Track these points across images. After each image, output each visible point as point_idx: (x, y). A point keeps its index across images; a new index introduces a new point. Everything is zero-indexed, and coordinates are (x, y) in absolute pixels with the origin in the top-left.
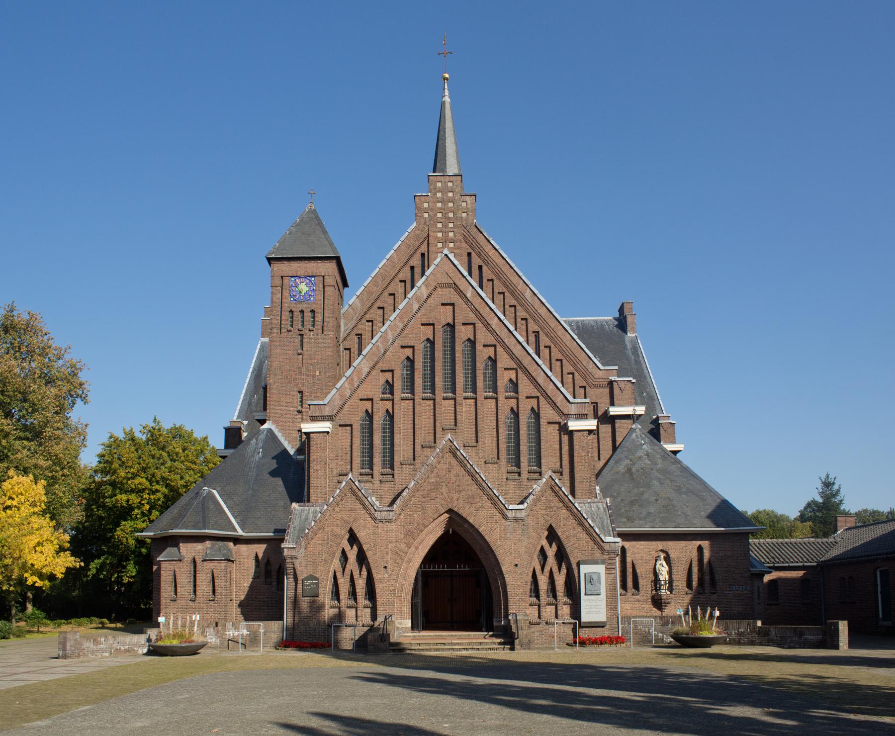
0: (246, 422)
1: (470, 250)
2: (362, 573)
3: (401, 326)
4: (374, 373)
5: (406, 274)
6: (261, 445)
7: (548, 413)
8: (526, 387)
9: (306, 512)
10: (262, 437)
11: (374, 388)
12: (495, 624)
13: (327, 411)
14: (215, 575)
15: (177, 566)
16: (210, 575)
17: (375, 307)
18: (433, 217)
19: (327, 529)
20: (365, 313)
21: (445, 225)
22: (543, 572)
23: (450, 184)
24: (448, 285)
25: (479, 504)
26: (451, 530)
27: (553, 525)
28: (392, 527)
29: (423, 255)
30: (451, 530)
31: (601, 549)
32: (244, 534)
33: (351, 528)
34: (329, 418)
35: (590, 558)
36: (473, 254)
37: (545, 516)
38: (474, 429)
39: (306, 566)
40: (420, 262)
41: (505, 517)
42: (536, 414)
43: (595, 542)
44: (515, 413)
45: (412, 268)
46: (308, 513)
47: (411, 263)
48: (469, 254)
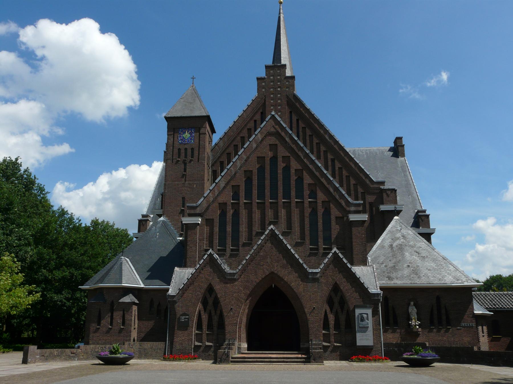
0: (152, 216)
5: (251, 125)
7: (335, 212)
9: (183, 273)
10: (159, 225)
12: (301, 346)
13: (198, 211)
20: (226, 149)
26: (273, 285)
27: (337, 282)
29: (262, 113)
30: (273, 285)
32: (144, 287)
37: (332, 277)
40: (259, 117)
42: (327, 213)
45: (255, 121)
46: (185, 274)
47: (255, 118)
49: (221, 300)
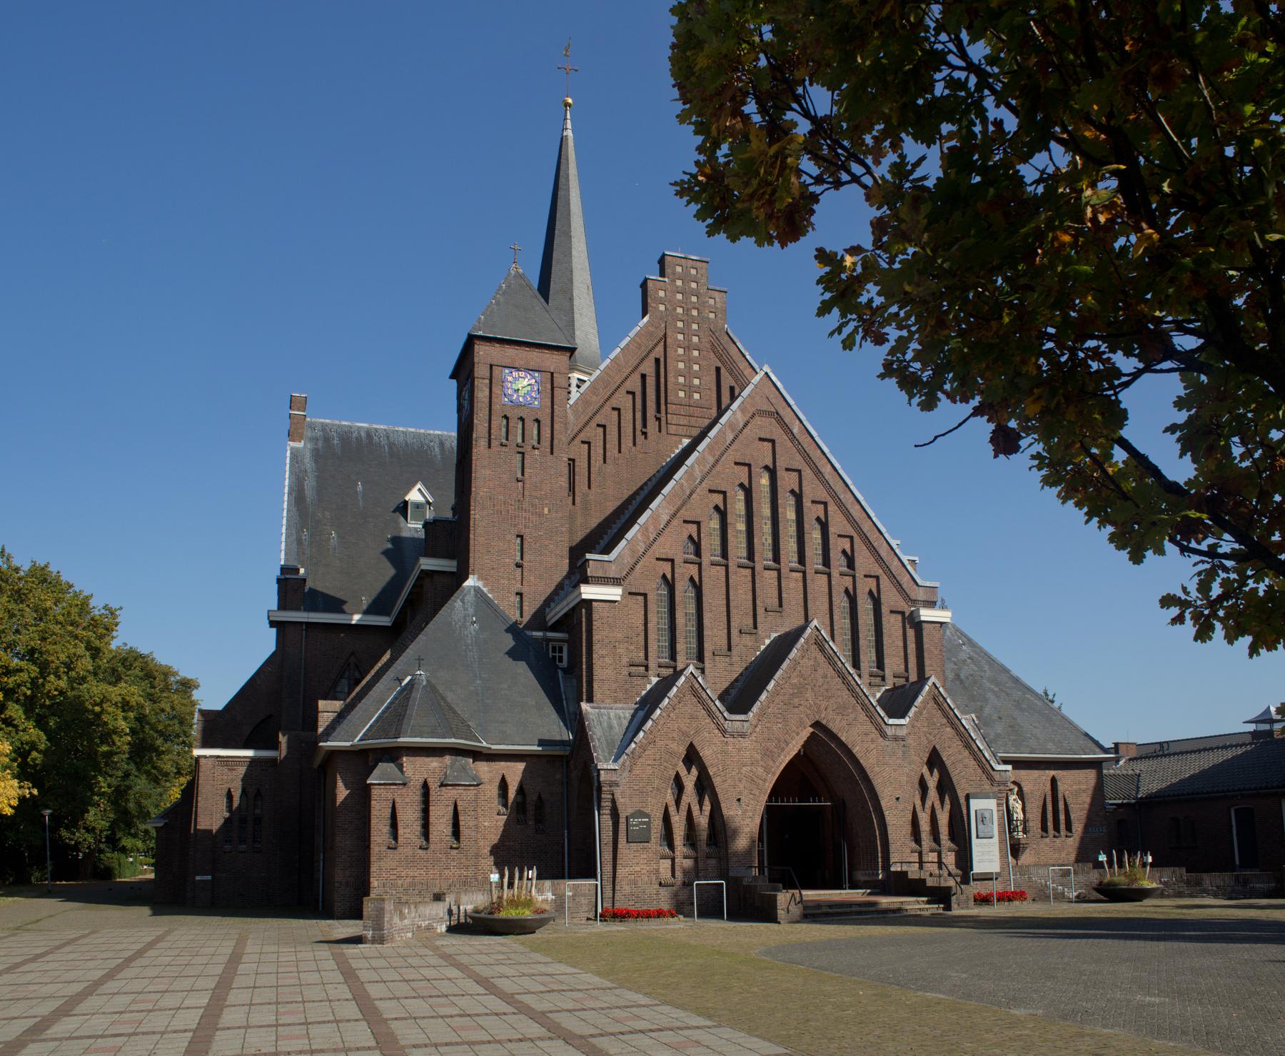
1: (719, 365)
2: (704, 808)
3: (711, 460)
4: (675, 522)
6: (471, 611)
7: (890, 598)
8: (864, 561)
11: (674, 544)
13: (613, 572)
14: (459, 808)
15: (465, 797)
16: (451, 809)
17: (593, 424)
18: (670, 312)
19: (659, 743)
20: (580, 431)
22: (924, 808)
23: (693, 272)
24: (770, 414)
25: (851, 716)
28: (745, 743)
29: (657, 361)
31: (990, 778)
33: (691, 743)
34: (615, 582)
35: (978, 790)
36: (723, 371)
38: (803, 613)
39: (631, 798)
41: (883, 735)
43: (984, 770)
44: (852, 599)
45: (643, 377)
46: (609, 718)
48: (718, 369)
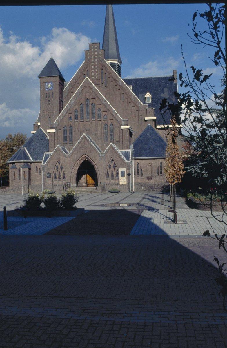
14: (25, 172)
18: (91, 58)
21: (95, 60)
29: (88, 70)
41: (99, 156)
49: (64, 166)
